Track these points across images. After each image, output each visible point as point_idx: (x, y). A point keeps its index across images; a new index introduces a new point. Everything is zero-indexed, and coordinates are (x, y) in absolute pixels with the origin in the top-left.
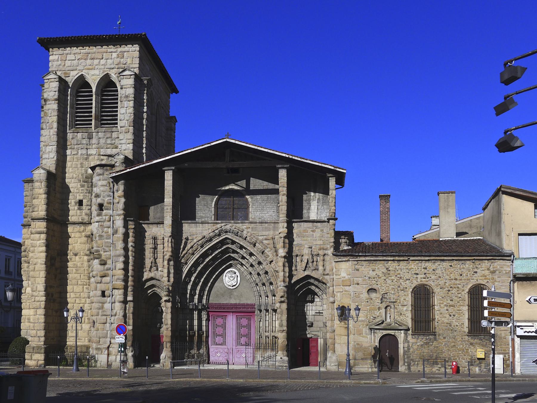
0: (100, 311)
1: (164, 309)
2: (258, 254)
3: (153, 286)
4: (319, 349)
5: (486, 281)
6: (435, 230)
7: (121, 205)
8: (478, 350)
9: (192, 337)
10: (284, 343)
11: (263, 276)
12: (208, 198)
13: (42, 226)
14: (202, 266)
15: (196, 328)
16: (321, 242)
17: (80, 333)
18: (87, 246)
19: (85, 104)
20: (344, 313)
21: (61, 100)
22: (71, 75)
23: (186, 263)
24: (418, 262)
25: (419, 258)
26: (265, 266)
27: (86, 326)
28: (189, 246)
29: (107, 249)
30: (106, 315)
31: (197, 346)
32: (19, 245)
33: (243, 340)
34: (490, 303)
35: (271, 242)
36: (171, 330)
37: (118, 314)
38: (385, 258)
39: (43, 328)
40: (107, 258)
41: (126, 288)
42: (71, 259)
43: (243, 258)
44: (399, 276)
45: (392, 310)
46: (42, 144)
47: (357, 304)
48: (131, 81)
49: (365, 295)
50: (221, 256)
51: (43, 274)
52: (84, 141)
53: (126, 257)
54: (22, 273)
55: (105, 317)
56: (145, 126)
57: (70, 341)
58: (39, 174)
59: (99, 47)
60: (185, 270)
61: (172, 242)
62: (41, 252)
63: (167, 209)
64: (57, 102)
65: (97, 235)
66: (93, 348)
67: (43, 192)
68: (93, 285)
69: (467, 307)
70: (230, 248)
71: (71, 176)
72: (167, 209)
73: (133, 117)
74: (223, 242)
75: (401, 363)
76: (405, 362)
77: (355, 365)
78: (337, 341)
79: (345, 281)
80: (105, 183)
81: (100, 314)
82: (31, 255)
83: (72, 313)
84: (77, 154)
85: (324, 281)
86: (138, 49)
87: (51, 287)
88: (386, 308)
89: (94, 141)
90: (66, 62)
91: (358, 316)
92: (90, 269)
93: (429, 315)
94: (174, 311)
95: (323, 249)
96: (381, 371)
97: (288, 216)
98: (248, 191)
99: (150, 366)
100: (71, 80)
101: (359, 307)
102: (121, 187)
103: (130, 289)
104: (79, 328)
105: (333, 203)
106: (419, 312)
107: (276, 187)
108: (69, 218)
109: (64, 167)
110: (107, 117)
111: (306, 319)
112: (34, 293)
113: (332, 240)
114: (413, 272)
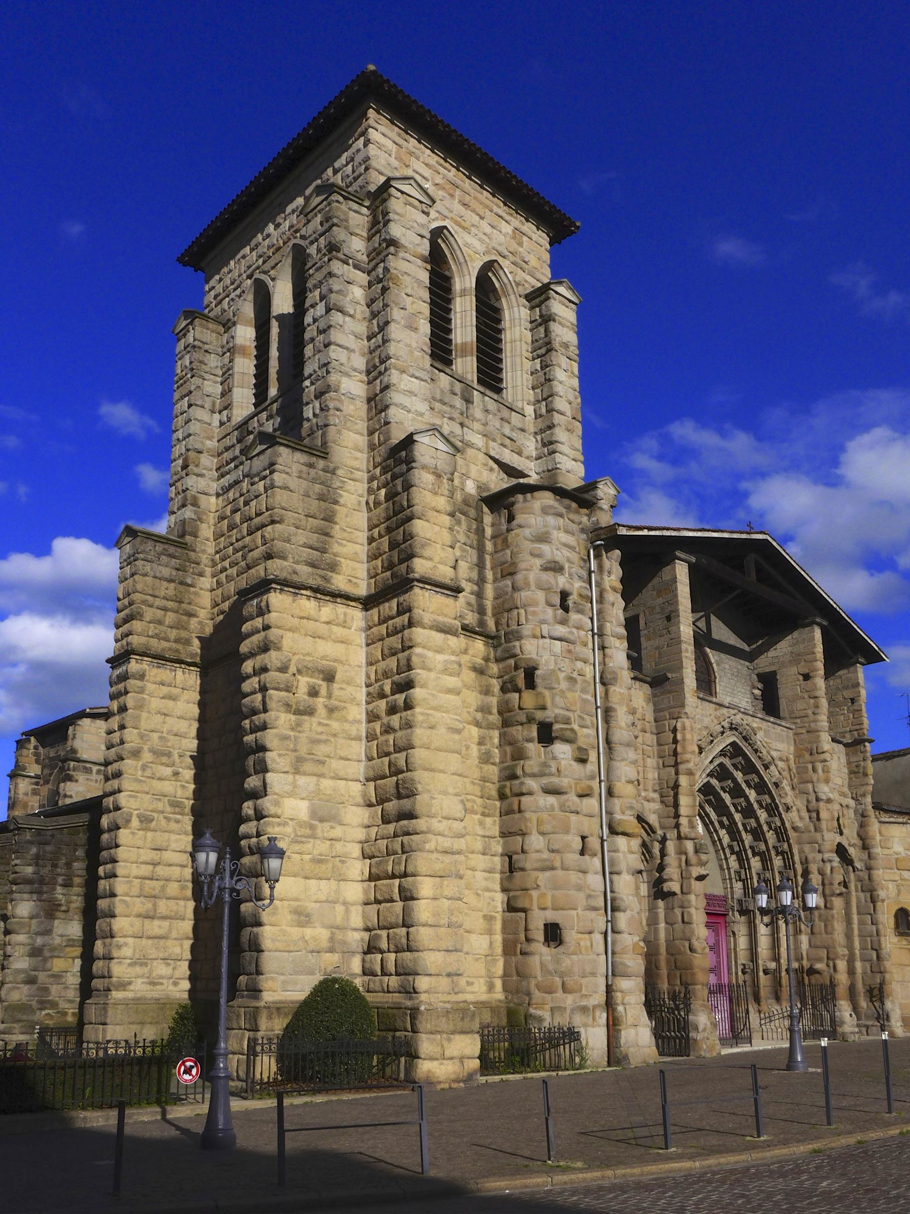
65: (562, 675)
89: (477, 411)
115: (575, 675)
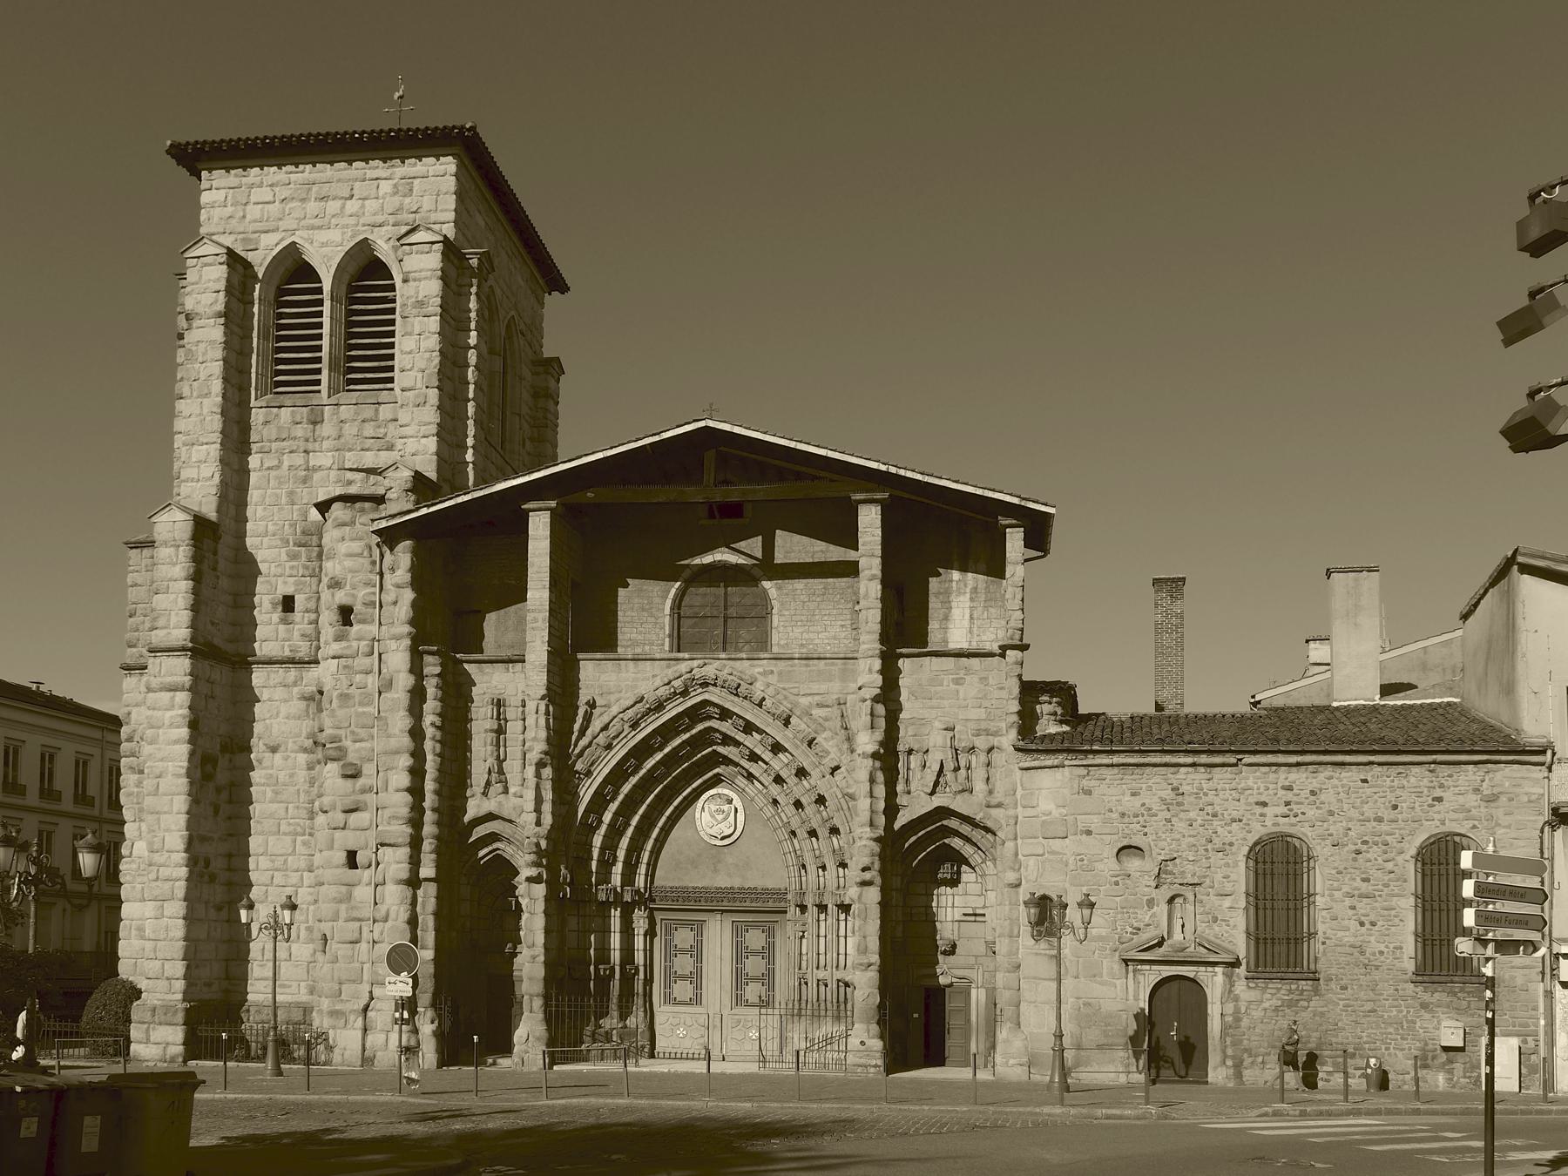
0: (343, 907)
1: (524, 902)
2: (797, 747)
3: (494, 837)
4: (973, 1018)
5: (1471, 823)
6: (1318, 677)
7: (404, 610)
8: (1444, 1024)
9: (604, 982)
10: (871, 1001)
11: (810, 809)
12: (653, 587)
13: (178, 668)
14: (634, 780)
15: (616, 956)
16: (982, 713)
17: (285, 969)
18: (307, 726)
19: (303, 326)
20: (1046, 914)
21: (235, 317)
22: (262, 245)
23: (589, 773)
24: (1266, 769)
25: (1270, 758)
26: (818, 781)
27: (301, 950)
28: (596, 725)
29: (362, 733)
30: (359, 920)
31: (620, 1007)
32: (114, 722)
33: (753, 991)
34: (1480, 889)
35: (836, 712)
36: (546, 963)
37: (392, 915)
38: (1168, 759)
39: (181, 954)
40: (361, 759)
41: (416, 843)
42: (260, 761)
43: (754, 757)
44: (1209, 809)
45: (1190, 907)
46: (179, 440)
47: (1085, 890)
48: (432, 260)
49: (1109, 865)
50: (688, 752)
51: (181, 803)
52: (299, 431)
53: (418, 755)
54: (123, 800)
55: (357, 924)
56: (472, 387)
57: (257, 992)
58: (172, 526)
59: (343, 164)
60: (587, 792)
61: (547, 713)
62: (176, 742)
63: (535, 620)
64: (222, 320)
65: (335, 694)
66: (320, 1011)
67: (183, 574)
68: (322, 835)
69: (1412, 900)
70: (717, 731)
71: (261, 529)
72: (535, 620)
73: (437, 361)
74: (695, 714)
75: (1214, 1058)
76: (1225, 1056)
77: (1077, 1064)
78: (1026, 994)
79: (1047, 822)
80: (356, 546)
81: (343, 915)
82: (147, 749)
83: (262, 913)
84: (278, 467)
85: (989, 824)
86: (453, 168)
87: (203, 839)
88: (1171, 900)
89: (327, 429)
90: (249, 207)
91: (1087, 923)
92: (315, 790)
93: (1297, 922)
94: (555, 907)
95: (988, 733)
96: (1154, 1082)
97: (884, 638)
98: (770, 568)
99: (485, 1063)
100: (261, 260)
101: (1092, 899)
102: (402, 558)
103: (428, 845)
104: (281, 954)
105: (1018, 601)
106: (1269, 912)
107: (851, 555)
108: (256, 645)
109: (242, 504)
110: (366, 362)
111: (935, 930)
112: (157, 858)
113: (1015, 706)
114: (1252, 800)
115: (352, 690)
